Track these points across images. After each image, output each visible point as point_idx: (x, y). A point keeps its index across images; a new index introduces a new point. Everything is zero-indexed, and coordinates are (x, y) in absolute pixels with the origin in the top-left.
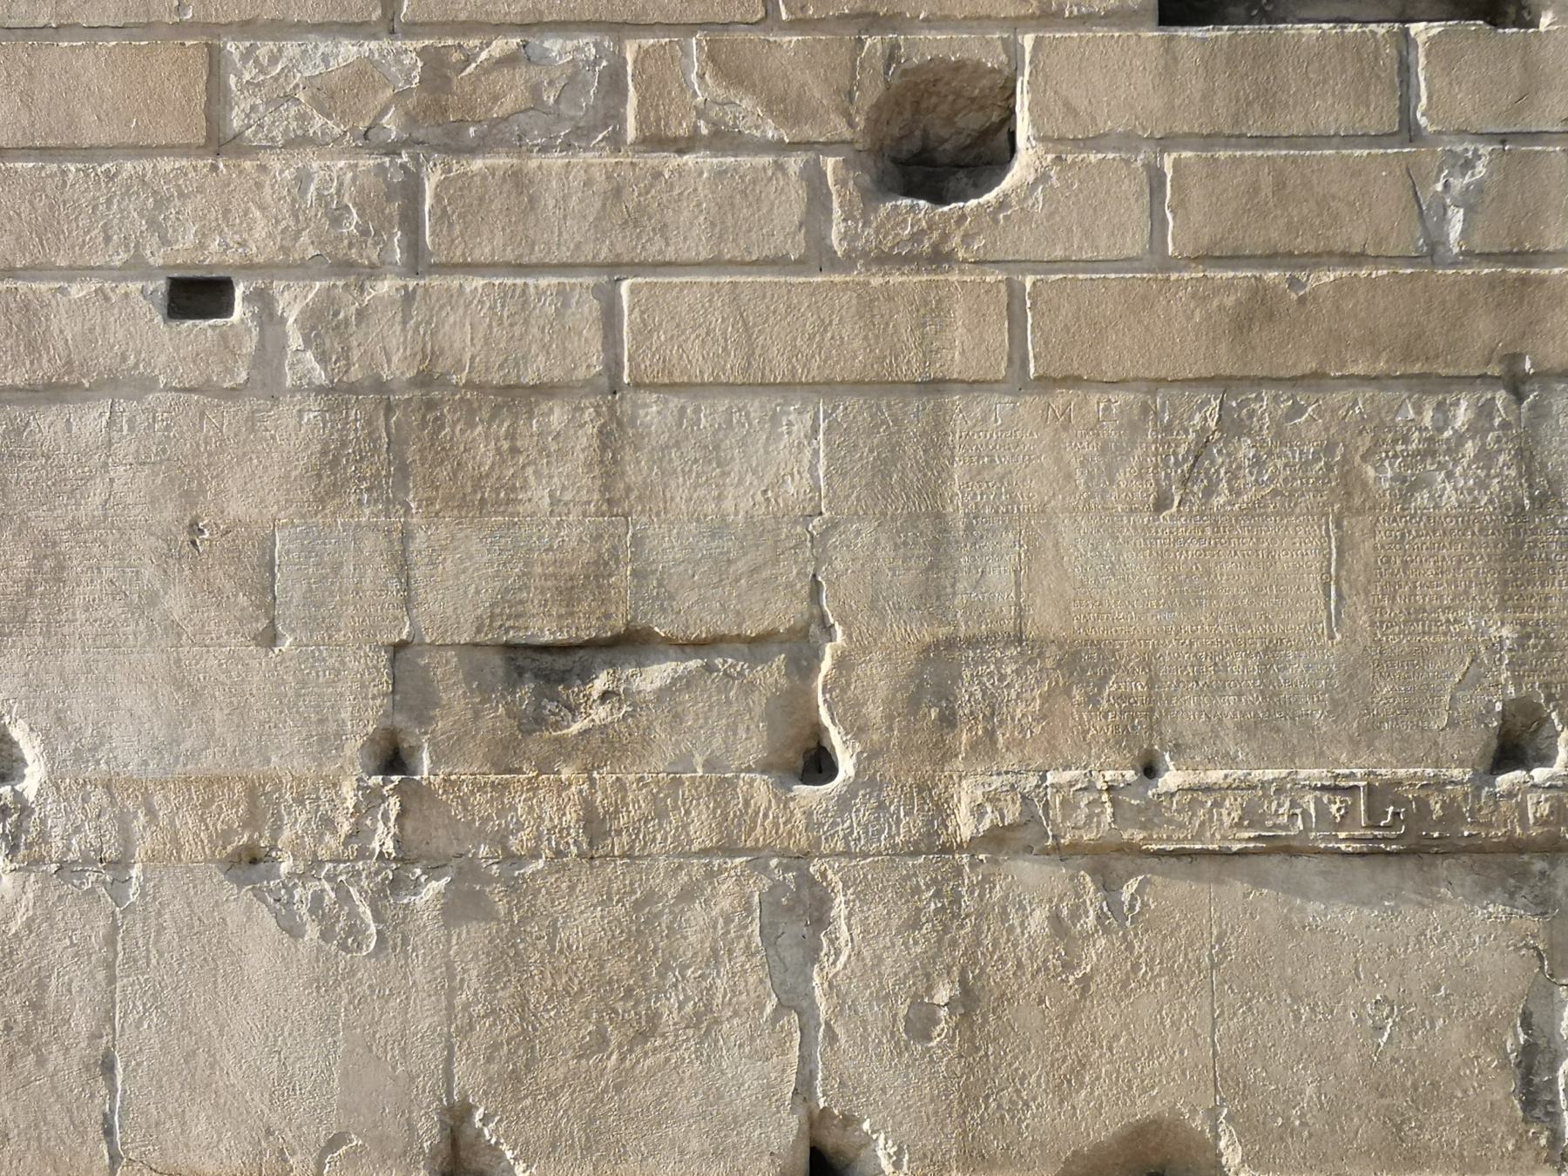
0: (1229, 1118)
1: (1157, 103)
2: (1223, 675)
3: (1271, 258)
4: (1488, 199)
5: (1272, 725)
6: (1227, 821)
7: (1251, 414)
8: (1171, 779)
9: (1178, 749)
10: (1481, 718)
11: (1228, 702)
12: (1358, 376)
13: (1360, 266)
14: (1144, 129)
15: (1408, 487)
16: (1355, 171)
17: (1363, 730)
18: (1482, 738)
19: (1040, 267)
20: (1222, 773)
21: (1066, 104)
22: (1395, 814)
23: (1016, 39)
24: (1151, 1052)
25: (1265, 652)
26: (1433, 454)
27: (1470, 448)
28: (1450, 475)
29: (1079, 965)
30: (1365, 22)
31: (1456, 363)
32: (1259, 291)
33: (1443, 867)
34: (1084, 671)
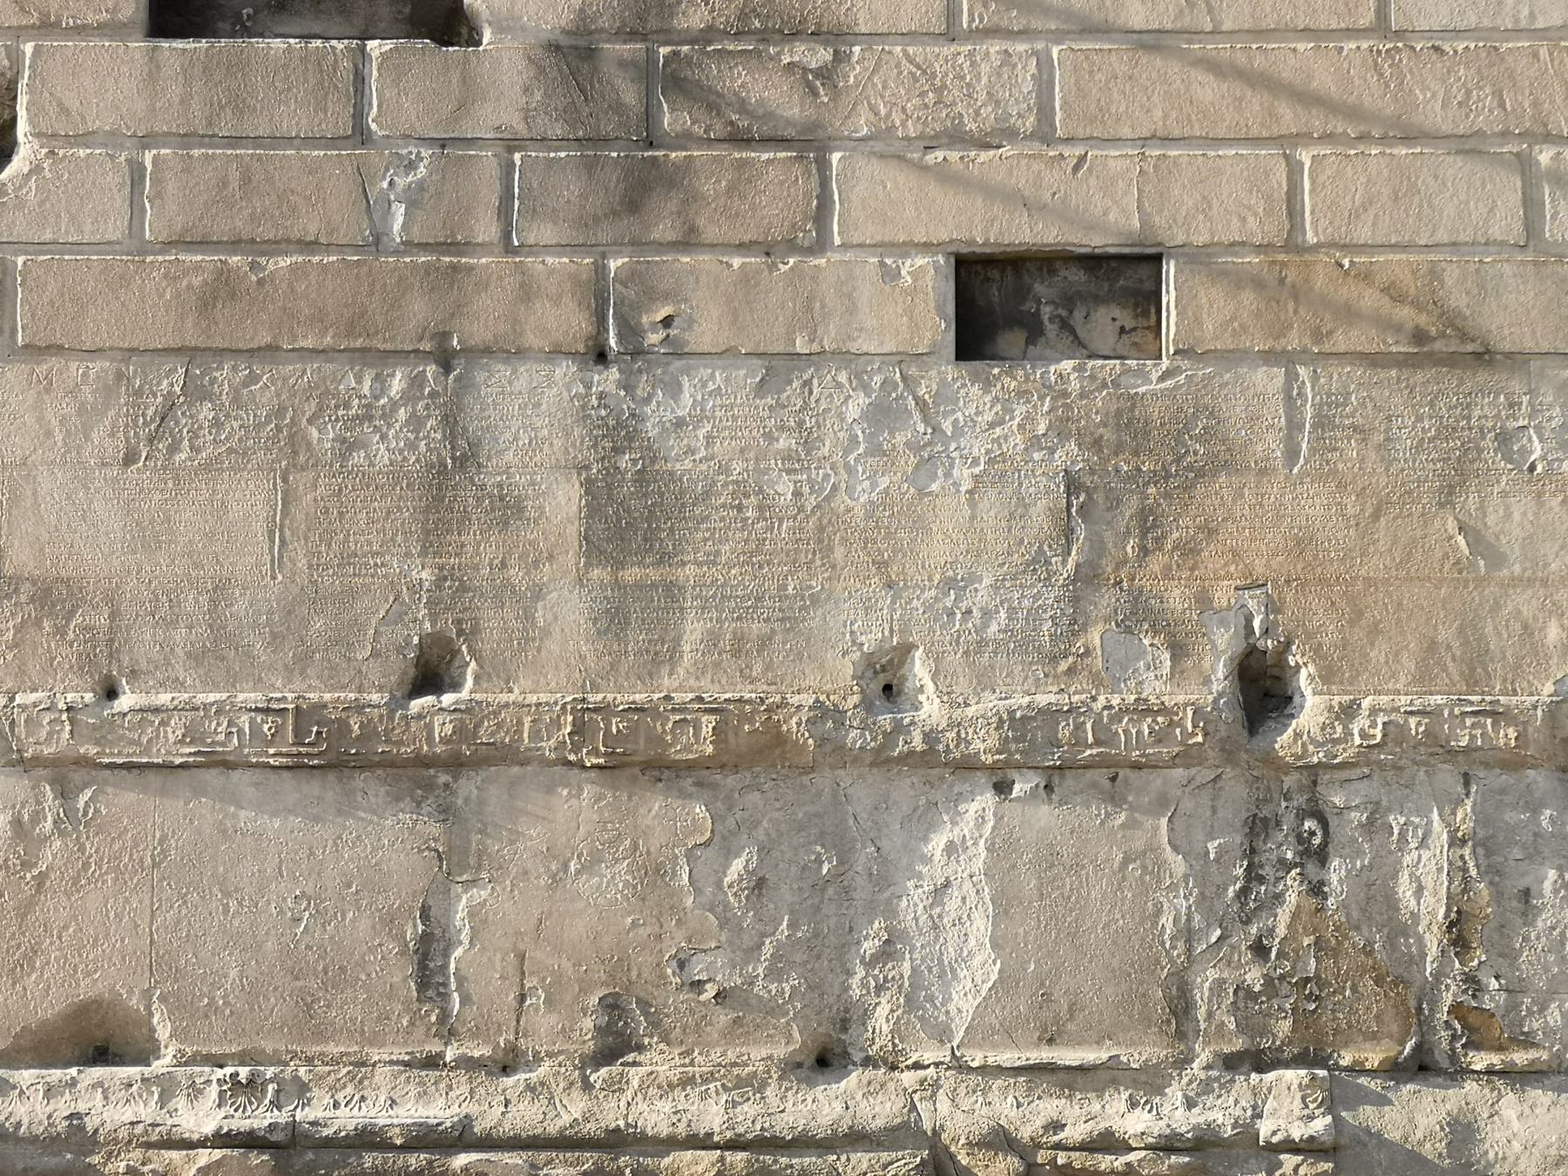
0: (162, 999)
1: (140, 106)
2: (176, 610)
3: (235, 245)
4: (427, 196)
5: (217, 654)
6: (172, 740)
7: (213, 381)
8: (125, 702)
9: (134, 675)
10: (400, 650)
11: (180, 634)
12: (307, 350)
13: (313, 253)
14: (128, 128)
15: (347, 447)
16: (312, 169)
17: (297, 659)
18: (400, 667)
19: (31, 248)
20: (169, 696)
21: (60, 104)
22: (319, 733)
23: (18, 48)
24: (96, 940)
25: (215, 589)
26: (370, 418)
27: (402, 414)
28: (383, 437)
29: (36, 864)
30: (327, 39)
31: (392, 339)
32: (224, 275)
33: (360, 780)
34: (54, 605)
